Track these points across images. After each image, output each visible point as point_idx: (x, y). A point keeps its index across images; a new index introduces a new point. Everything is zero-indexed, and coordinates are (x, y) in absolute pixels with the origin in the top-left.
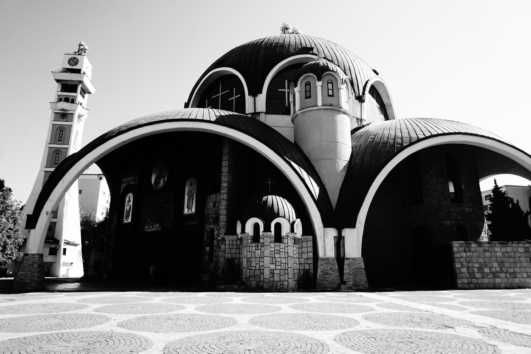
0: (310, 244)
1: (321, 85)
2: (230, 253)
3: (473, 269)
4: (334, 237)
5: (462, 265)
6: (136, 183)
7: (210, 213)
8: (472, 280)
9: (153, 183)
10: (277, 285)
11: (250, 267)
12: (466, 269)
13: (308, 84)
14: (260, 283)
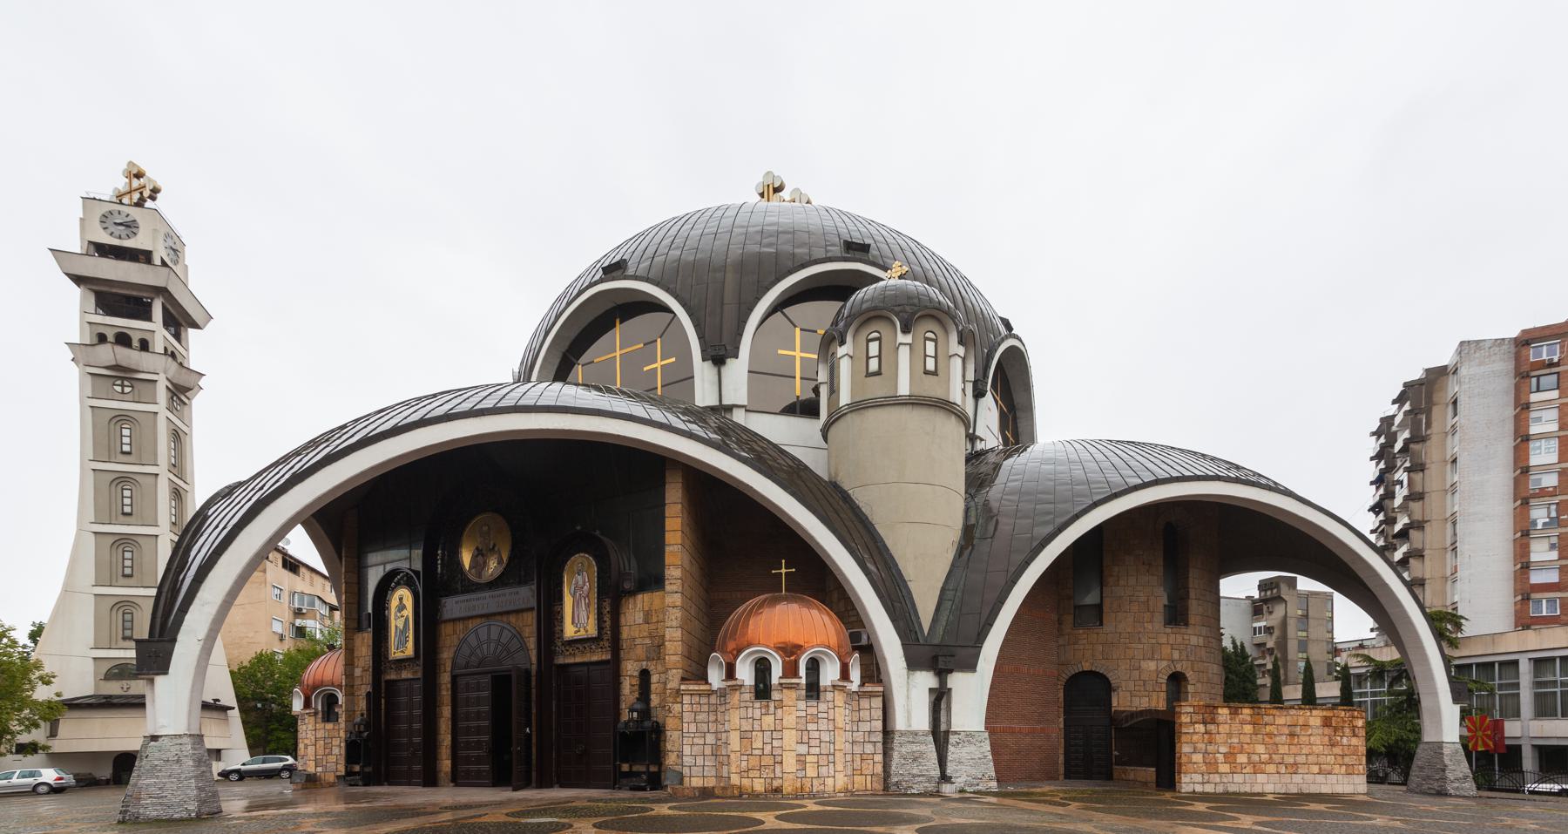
0: (877, 703)
3: (1216, 759)
4: (930, 689)
5: (1195, 748)
6: (418, 566)
8: (1211, 776)
10: (812, 786)
12: (1201, 755)
14: (774, 782)
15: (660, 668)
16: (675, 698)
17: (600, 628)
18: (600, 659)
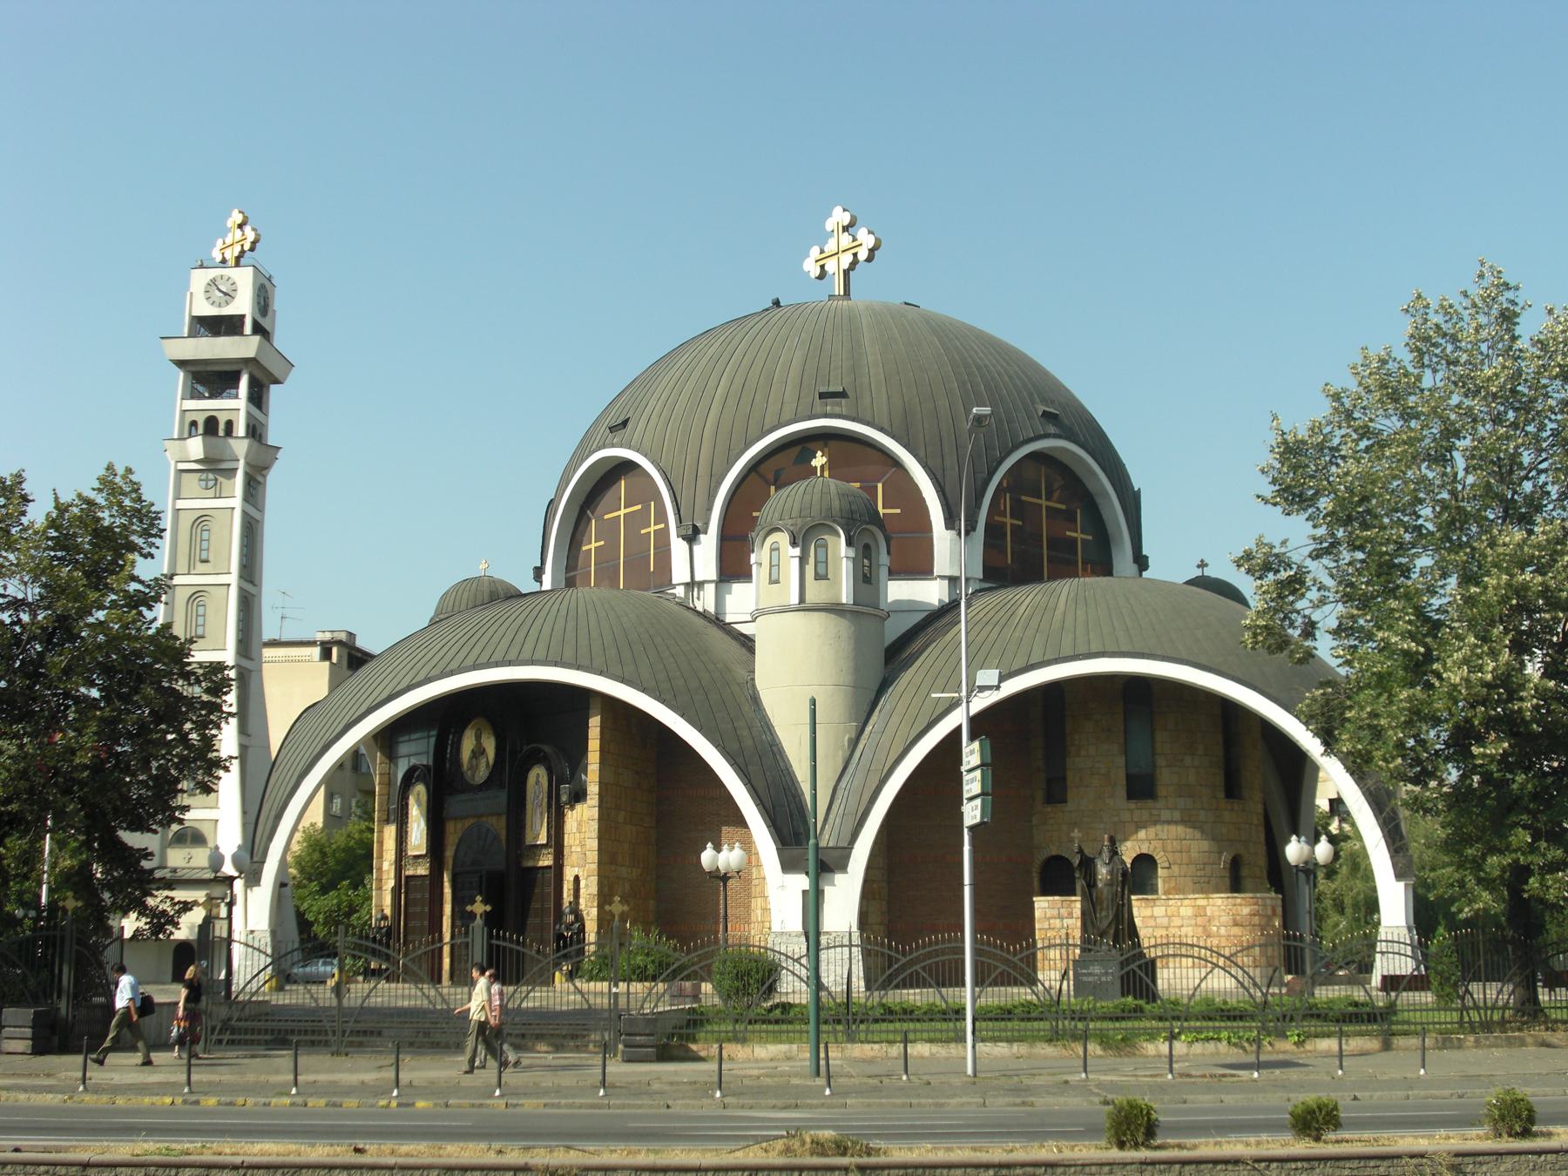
1: (798, 554)
6: (431, 763)
9: (465, 767)
13: (775, 549)
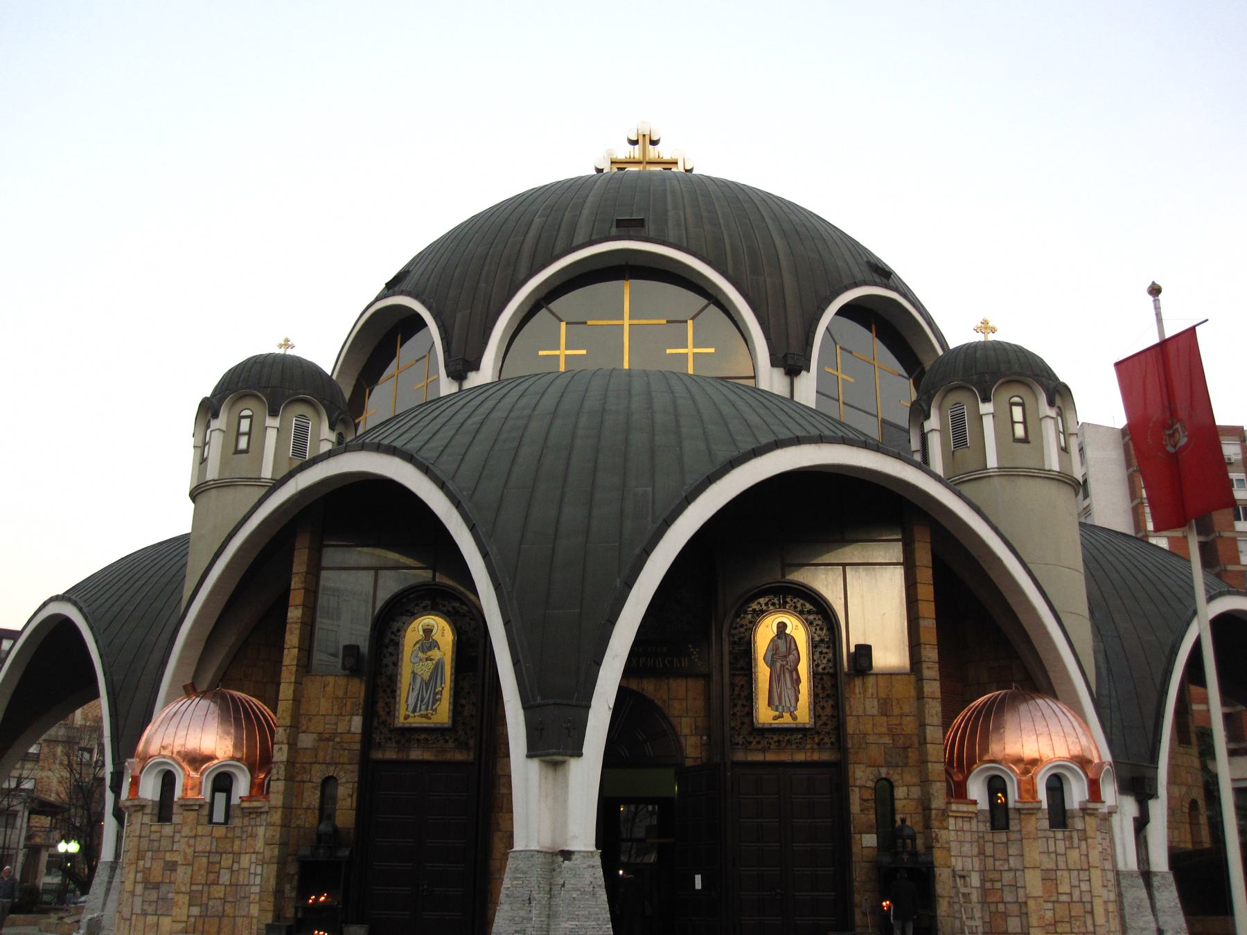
2: (961, 856)
7: (870, 731)
11: (1055, 894)
15: (908, 778)
16: (941, 821)
17: (817, 717)
18: (808, 759)
